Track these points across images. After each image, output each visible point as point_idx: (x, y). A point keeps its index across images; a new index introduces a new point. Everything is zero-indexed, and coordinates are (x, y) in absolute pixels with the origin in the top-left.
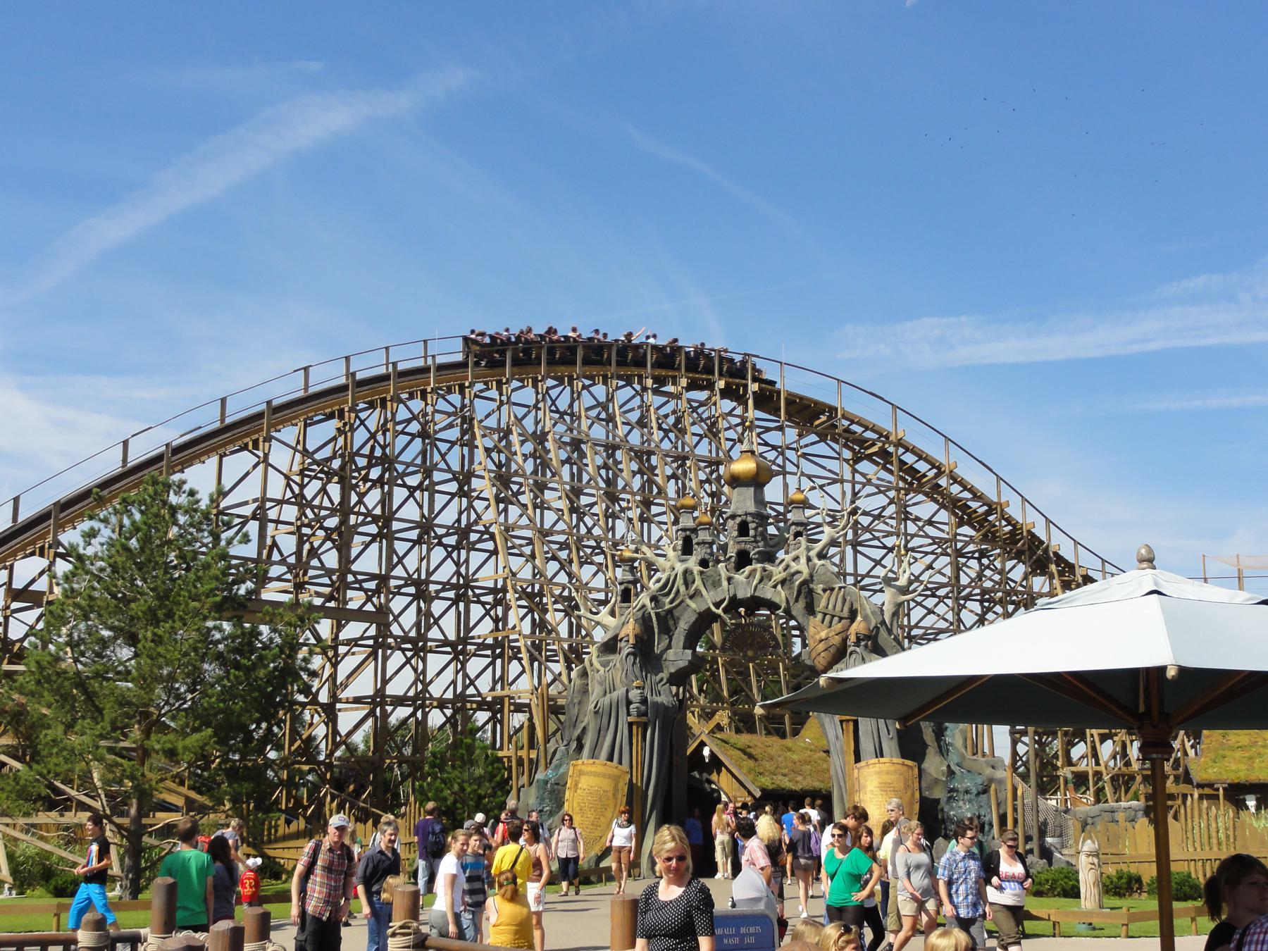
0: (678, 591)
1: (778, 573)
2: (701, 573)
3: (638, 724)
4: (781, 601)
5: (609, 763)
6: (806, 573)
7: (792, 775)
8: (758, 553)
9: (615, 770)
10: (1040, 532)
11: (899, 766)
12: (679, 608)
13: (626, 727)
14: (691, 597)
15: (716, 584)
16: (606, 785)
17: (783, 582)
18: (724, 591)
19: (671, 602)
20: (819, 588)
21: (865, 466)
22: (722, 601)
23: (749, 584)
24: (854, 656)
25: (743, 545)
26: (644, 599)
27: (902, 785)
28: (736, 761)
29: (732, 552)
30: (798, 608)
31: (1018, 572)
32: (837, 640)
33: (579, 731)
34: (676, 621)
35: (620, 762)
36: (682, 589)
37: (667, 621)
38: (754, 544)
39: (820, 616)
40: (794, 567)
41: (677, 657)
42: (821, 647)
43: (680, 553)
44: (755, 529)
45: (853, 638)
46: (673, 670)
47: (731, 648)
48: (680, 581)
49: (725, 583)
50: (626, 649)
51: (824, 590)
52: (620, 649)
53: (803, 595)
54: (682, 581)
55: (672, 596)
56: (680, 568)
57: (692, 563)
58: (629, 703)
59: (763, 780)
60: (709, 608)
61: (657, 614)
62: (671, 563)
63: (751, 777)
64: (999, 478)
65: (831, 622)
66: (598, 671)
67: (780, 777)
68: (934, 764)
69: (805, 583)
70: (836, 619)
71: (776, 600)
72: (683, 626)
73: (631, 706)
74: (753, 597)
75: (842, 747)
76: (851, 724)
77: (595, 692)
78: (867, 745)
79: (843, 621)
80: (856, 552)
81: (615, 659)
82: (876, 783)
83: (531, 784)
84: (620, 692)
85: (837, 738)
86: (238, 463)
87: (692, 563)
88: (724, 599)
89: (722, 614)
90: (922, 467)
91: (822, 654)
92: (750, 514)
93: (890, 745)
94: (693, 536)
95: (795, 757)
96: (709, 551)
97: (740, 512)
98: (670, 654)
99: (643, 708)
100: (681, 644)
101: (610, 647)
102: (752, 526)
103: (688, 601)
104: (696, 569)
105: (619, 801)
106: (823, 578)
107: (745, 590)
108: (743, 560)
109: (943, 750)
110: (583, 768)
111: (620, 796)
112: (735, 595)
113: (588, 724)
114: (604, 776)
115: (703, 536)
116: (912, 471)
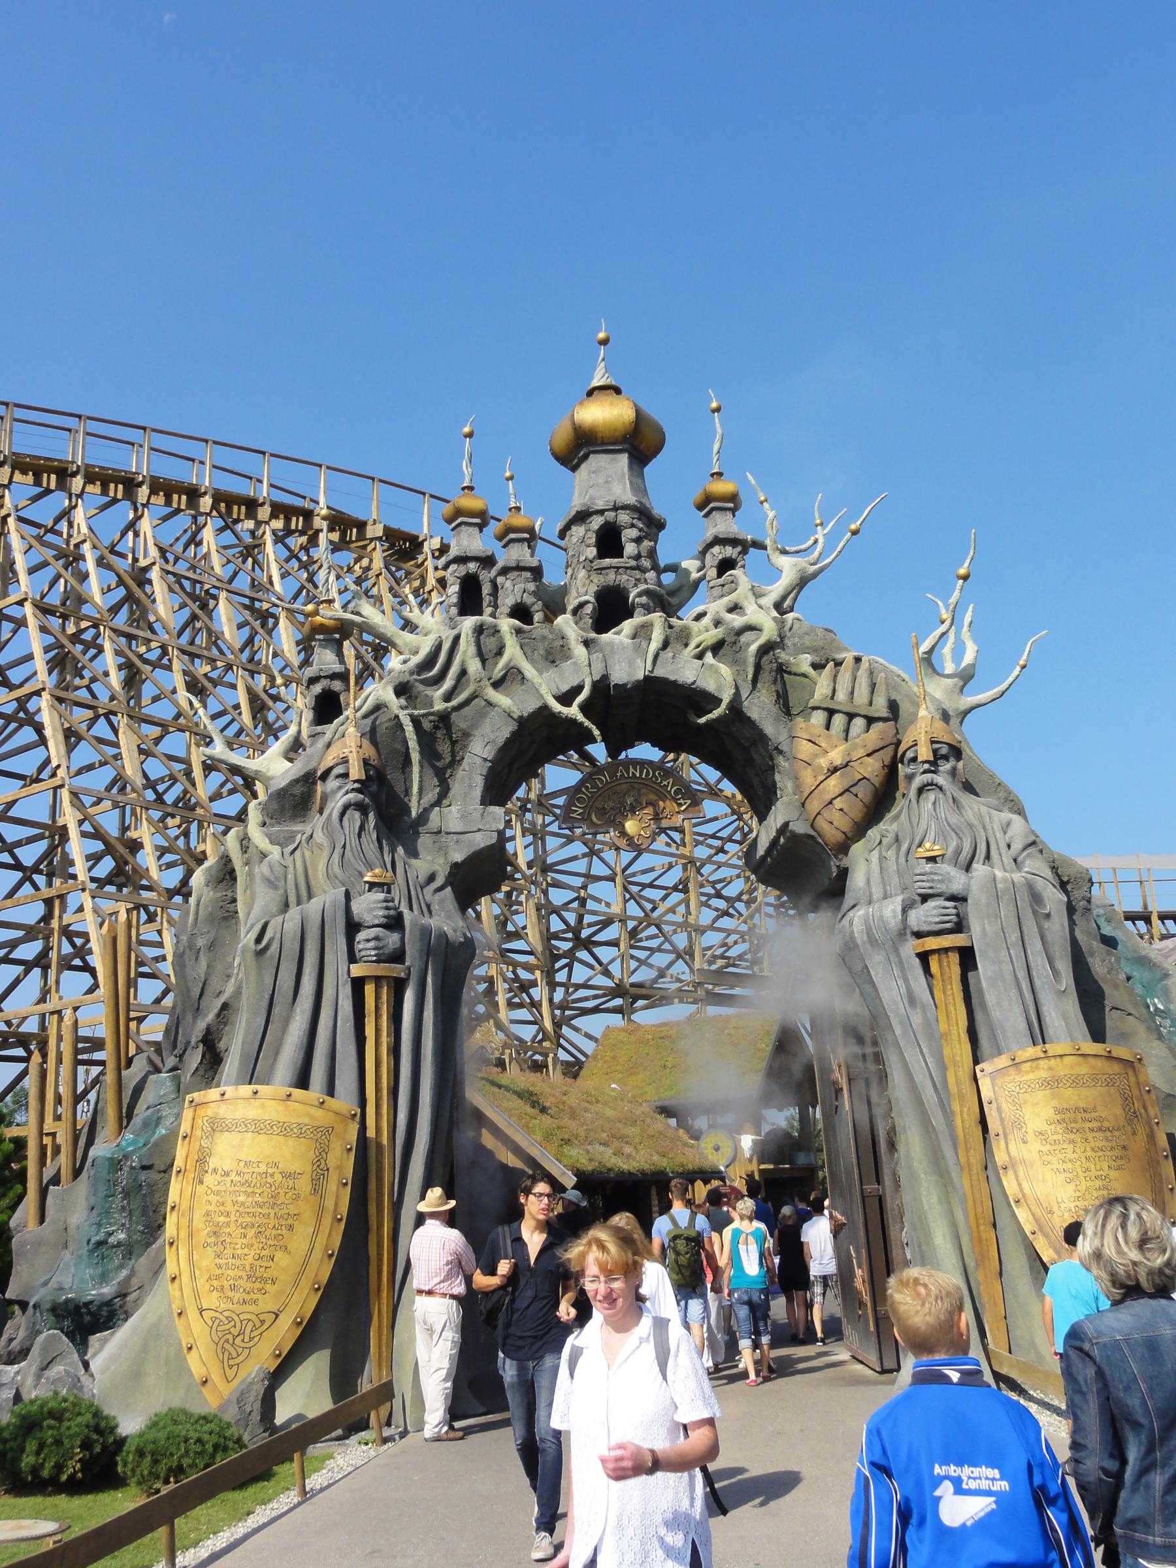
0: (463, 673)
2: (518, 631)
3: (377, 980)
4: (720, 688)
5: (298, 1093)
6: (769, 630)
7: (616, 1143)
8: (647, 593)
9: (318, 1113)
11: (1099, 1064)
12: (466, 711)
13: (346, 991)
14: (497, 685)
15: (555, 655)
17: (717, 648)
19: (448, 698)
20: (804, 663)
22: (579, 689)
23: (640, 651)
24: (931, 796)
25: (612, 575)
27: (1119, 1111)
28: (520, 1118)
32: (872, 768)
33: (210, 1016)
34: (459, 742)
35: (331, 1092)
36: (474, 666)
38: (637, 574)
39: (819, 718)
42: (834, 785)
43: (454, 611)
44: (638, 541)
45: (925, 753)
46: (459, 857)
47: (586, 819)
48: (467, 647)
49: (580, 651)
50: (338, 795)
51: (817, 666)
52: (325, 799)
53: (765, 676)
54: (472, 650)
55: (448, 683)
58: (353, 927)
59: (574, 1153)
60: (545, 708)
61: (416, 721)
63: (554, 1147)
65: (847, 731)
66: (264, 855)
67: (602, 1148)
69: (767, 649)
70: (859, 722)
71: (709, 684)
73: (361, 936)
74: (647, 679)
75: (927, 1024)
76: (954, 958)
79: (877, 727)
81: (316, 825)
82: (1048, 1112)
83: (77, 1173)
84: (328, 897)
85: (912, 999)
88: (579, 689)
89: (580, 717)
91: (838, 803)
92: (625, 507)
94: (485, 576)
95: (608, 1112)
96: (532, 587)
97: (600, 505)
98: (452, 816)
99: (393, 939)
100: (478, 793)
102: (629, 534)
103: (492, 694)
105: (330, 1203)
106: (807, 641)
107: (631, 664)
110: (223, 1110)
111: (333, 1186)
112: (605, 678)
113: (238, 993)
114: (285, 1130)
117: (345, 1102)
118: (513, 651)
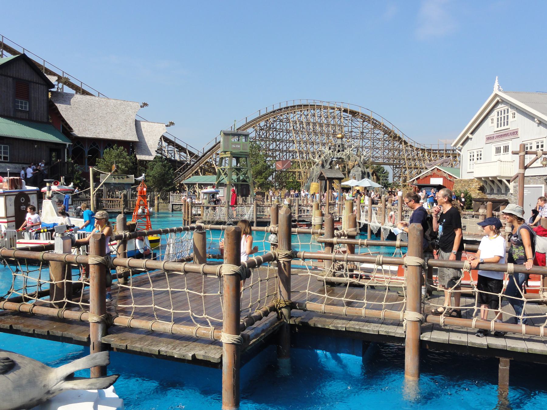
1: (344, 153)
10: (401, 136)
16: (317, 186)
21: (365, 123)
29: (337, 150)
31: (397, 144)
37: (326, 161)
40: (347, 153)
56: (329, 152)
57: (331, 151)
62: (327, 151)
72: (329, 162)
80: (363, 141)
87: (331, 151)
101: (318, 165)
108: (339, 151)
116: (375, 123)
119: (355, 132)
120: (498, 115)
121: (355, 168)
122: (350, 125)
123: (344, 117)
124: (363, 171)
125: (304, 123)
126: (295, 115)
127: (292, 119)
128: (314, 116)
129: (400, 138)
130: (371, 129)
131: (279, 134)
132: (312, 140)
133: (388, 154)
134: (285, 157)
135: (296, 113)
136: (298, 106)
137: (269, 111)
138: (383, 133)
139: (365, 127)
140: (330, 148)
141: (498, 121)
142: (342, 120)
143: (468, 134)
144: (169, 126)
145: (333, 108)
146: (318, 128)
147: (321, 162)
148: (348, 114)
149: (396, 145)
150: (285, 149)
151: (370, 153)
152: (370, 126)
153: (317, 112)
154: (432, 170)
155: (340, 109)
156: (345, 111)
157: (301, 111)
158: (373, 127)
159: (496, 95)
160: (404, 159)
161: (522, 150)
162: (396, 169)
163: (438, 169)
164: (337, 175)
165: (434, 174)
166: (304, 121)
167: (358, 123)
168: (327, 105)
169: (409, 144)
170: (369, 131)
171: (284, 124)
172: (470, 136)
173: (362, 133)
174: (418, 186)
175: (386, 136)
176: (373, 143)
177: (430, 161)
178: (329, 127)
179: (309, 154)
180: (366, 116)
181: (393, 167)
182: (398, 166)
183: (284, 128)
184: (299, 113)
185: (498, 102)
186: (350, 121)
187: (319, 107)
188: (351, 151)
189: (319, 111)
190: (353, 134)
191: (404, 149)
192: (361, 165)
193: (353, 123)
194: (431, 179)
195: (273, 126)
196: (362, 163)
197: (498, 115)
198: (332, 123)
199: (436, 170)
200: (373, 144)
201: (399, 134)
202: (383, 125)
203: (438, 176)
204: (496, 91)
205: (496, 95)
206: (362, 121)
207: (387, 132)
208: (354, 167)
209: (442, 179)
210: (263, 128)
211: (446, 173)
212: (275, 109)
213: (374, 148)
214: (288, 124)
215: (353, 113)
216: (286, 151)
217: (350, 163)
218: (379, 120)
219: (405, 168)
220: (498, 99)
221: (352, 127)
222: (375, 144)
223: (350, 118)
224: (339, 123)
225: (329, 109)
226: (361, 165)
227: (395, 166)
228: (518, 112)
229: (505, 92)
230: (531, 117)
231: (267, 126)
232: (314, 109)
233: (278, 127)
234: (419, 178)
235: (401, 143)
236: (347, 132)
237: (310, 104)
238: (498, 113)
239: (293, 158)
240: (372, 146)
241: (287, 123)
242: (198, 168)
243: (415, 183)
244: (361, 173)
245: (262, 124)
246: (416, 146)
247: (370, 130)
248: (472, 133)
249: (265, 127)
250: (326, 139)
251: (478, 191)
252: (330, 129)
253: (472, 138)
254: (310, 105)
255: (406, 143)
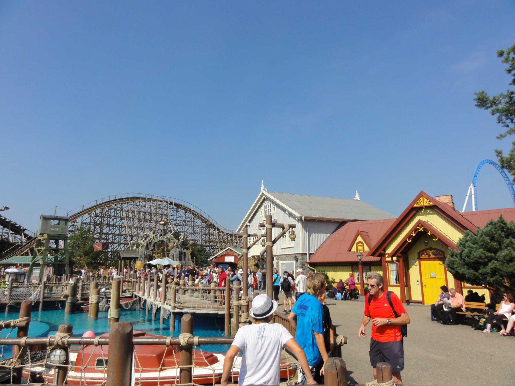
1: (166, 237)
10: (215, 224)
15: (157, 238)
16: (141, 264)
18: (158, 239)
21: (187, 214)
26: (147, 240)
30: (168, 242)
32: (172, 246)
37: (150, 243)
40: (168, 236)
41: (151, 248)
48: (152, 238)
56: (153, 236)
62: (151, 234)
64: (209, 216)
68: (183, 262)
72: (153, 244)
77: (140, 252)
78: (175, 259)
80: (185, 227)
84: (144, 252)
86: (86, 216)
87: (155, 235)
90: (197, 214)
93: (178, 259)
98: (151, 247)
101: (143, 246)
104: (155, 236)
108: (161, 235)
109: (185, 260)
115: (156, 232)
117: (144, 262)
118: (155, 238)
119: (179, 220)
120: (265, 209)
121: (174, 249)
122: (175, 214)
123: (170, 209)
124: (181, 251)
125: (135, 212)
126: (128, 205)
127: (126, 209)
128: (145, 206)
129: (214, 226)
130: (192, 218)
131: (113, 220)
132: (143, 226)
133: (205, 237)
134: (117, 240)
135: (129, 204)
136: (131, 198)
137: (104, 201)
138: (201, 222)
139: (187, 217)
140: (154, 232)
141: (265, 213)
142: (169, 211)
143: (247, 223)
144: (3, 210)
145: (161, 201)
146: (148, 217)
147: (145, 244)
148: (173, 206)
149: (211, 231)
150: (117, 232)
151: (190, 237)
152: (191, 216)
153: (148, 203)
154: (226, 250)
155: (167, 202)
156: (171, 203)
157: (133, 202)
158: (193, 217)
159: (263, 194)
160: (217, 242)
161: (245, 233)
162: (212, 250)
163: (230, 250)
164: (132, 255)
165: (228, 253)
166: (136, 210)
167: (182, 213)
168: (156, 198)
169: (220, 231)
170: (190, 220)
171: (118, 212)
172: (248, 224)
173: (185, 221)
174: (215, 263)
175: (204, 224)
176: (194, 229)
177: (237, 243)
178: (157, 216)
179: (138, 237)
180: (187, 208)
181: (209, 248)
182: (213, 247)
183: (117, 216)
184: (132, 203)
185: (264, 200)
186: (175, 212)
187: (149, 199)
188: (172, 235)
189: (149, 202)
190: (178, 222)
191: (217, 234)
192: (179, 246)
193: (177, 213)
194: (226, 257)
195: (108, 213)
196: (180, 245)
197: (265, 209)
198: (160, 212)
199: (229, 251)
200: (193, 230)
201: (213, 223)
202: (201, 215)
203: (230, 255)
204: (262, 191)
205: (263, 194)
206: (185, 212)
207: (204, 220)
208: (173, 248)
209: (234, 257)
210: (98, 214)
211: (236, 253)
212: (111, 199)
213: (194, 233)
214: (122, 212)
215: (178, 206)
216: (118, 234)
217: (170, 245)
218: (197, 211)
219: (218, 249)
220: (264, 196)
221: (176, 216)
222: (195, 230)
223: (174, 209)
224: (166, 213)
225: (157, 202)
226: (179, 246)
227: (210, 247)
228: (276, 207)
229: (268, 192)
230: (284, 210)
231: (102, 212)
232: (145, 201)
233: (112, 214)
234: (216, 257)
235: (215, 230)
236: (172, 220)
237: (142, 197)
238: (265, 207)
239: (125, 240)
240: (193, 231)
241: (121, 211)
242: (28, 249)
243: (213, 261)
244: (178, 252)
245: (98, 211)
246: (226, 232)
247: (191, 219)
248: (250, 222)
249: (101, 214)
250: (137, 223)
251: (254, 267)
252: (158, 217)
253: (249, 226)
254: (142, 198)
255: (218, 229)
